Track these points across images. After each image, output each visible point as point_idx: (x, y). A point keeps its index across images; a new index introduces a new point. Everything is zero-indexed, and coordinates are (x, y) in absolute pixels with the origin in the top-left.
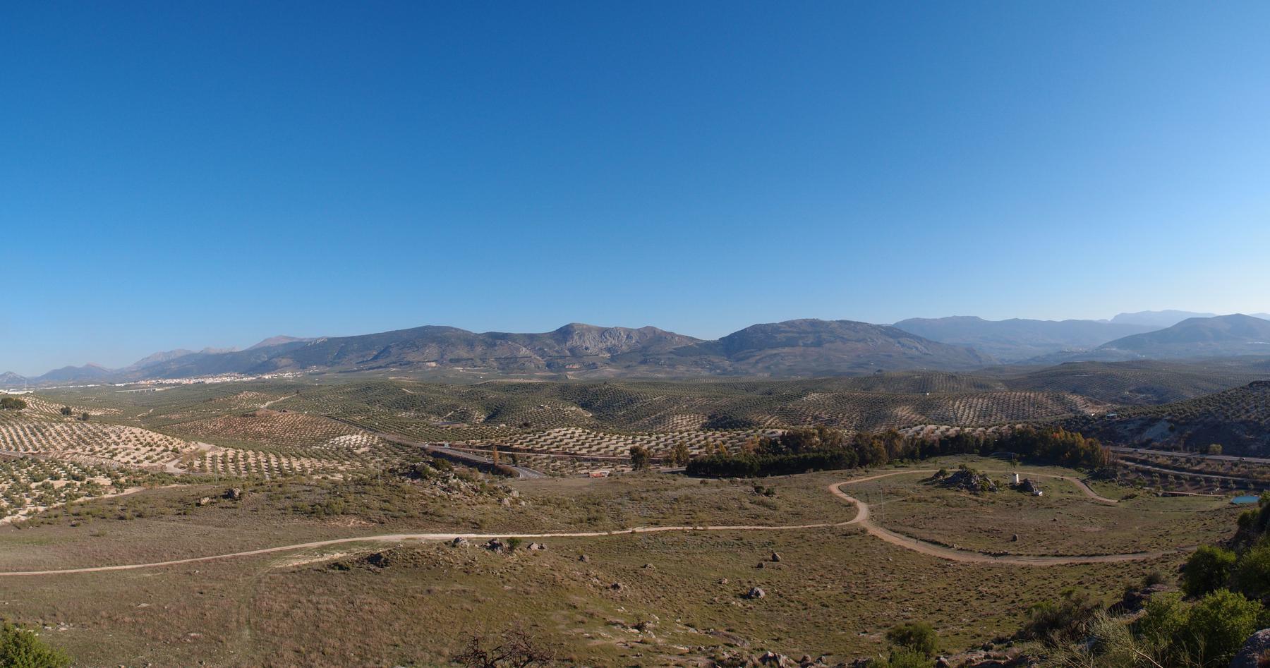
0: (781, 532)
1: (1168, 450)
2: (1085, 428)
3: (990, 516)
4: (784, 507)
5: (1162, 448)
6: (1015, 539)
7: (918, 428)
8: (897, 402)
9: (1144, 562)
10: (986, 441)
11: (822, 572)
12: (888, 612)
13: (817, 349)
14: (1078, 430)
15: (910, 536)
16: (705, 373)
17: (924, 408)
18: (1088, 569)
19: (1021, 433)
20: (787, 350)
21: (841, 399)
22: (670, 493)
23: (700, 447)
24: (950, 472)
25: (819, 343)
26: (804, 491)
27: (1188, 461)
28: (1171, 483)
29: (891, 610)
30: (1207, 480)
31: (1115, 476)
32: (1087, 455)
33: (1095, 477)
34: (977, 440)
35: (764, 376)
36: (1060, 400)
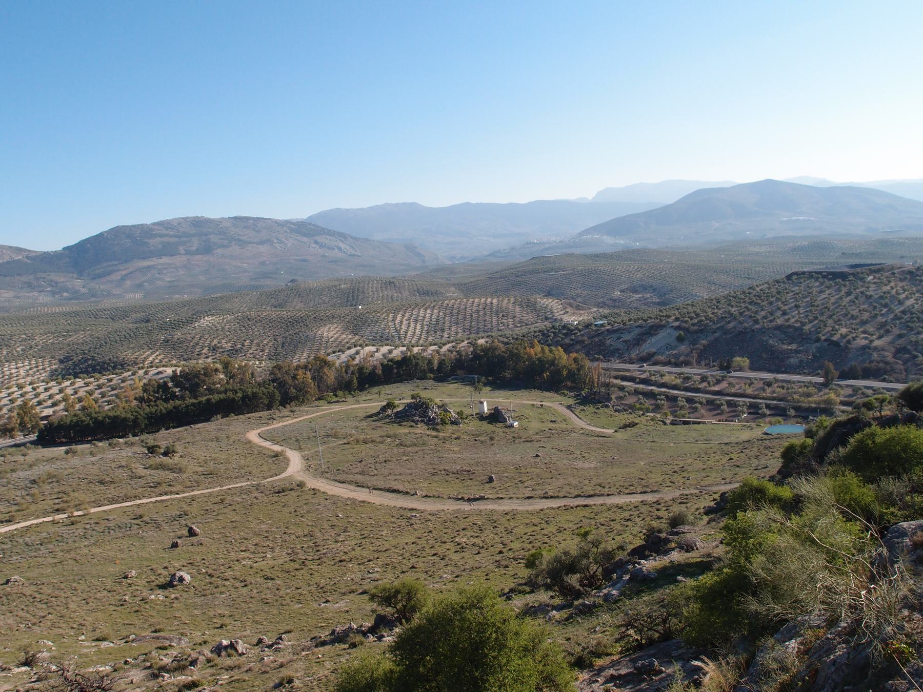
0: (193, 499)
1: (676, 365)
2: (567, 341)
3: (457, 455)
4: (192, 467)
5: (665, 364)
6: (491, 480)
7: (353, 351)
8: (321, 320)
9: (658, 503)
10: (441, 363)
11: (256, 540)
12: (349, 576)
13: (205, 258)
14: (557, 344)
15: (360, 485)
16: (43, 298)
17: (356, 325)
18: (587, 512)
19: (486, 350)
20: (165, 260)
21: (245, 322)
22: (21, 474)
23: (54, 405)
24: (401, 404)
25: (207, 249)
26: (215, 443)
27: (704, 379)
28: (682, 408)
29: (354, 573)
30: (729, 404)
31: (609, 399)
32: (572, 376)
33: (585, 401)
34: (430, 362)
35: (136, 297)
36: (531, 306)
